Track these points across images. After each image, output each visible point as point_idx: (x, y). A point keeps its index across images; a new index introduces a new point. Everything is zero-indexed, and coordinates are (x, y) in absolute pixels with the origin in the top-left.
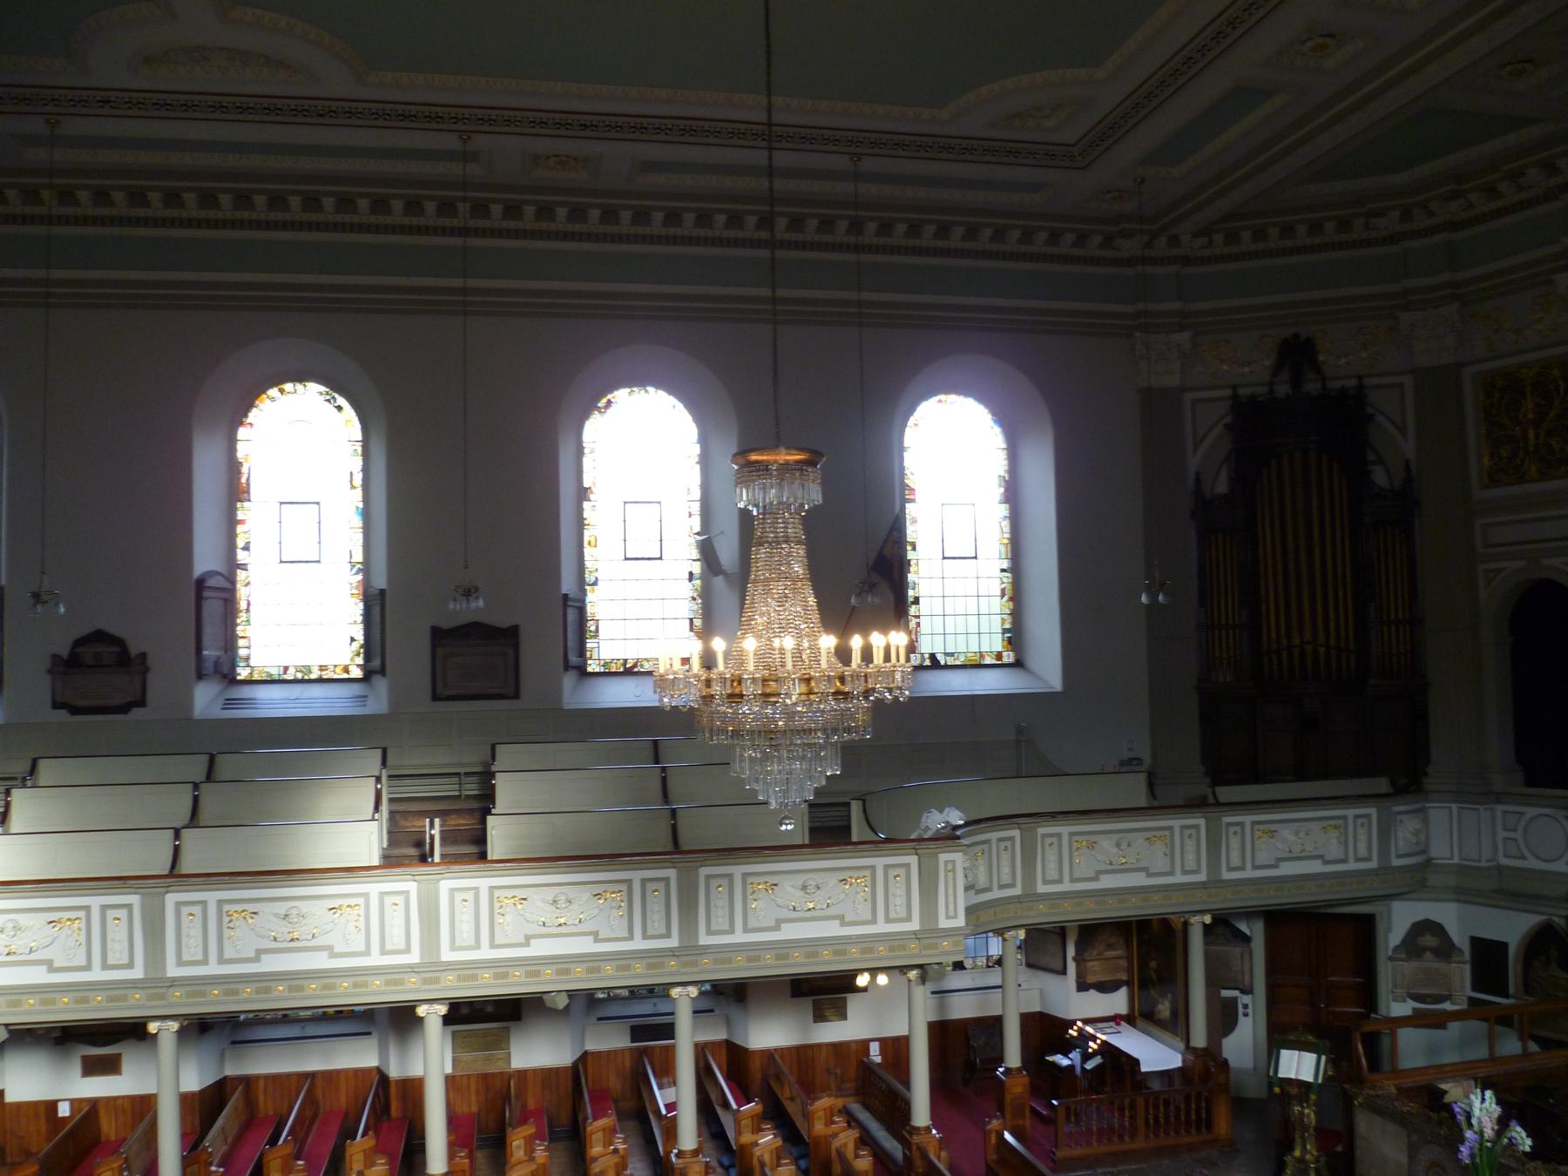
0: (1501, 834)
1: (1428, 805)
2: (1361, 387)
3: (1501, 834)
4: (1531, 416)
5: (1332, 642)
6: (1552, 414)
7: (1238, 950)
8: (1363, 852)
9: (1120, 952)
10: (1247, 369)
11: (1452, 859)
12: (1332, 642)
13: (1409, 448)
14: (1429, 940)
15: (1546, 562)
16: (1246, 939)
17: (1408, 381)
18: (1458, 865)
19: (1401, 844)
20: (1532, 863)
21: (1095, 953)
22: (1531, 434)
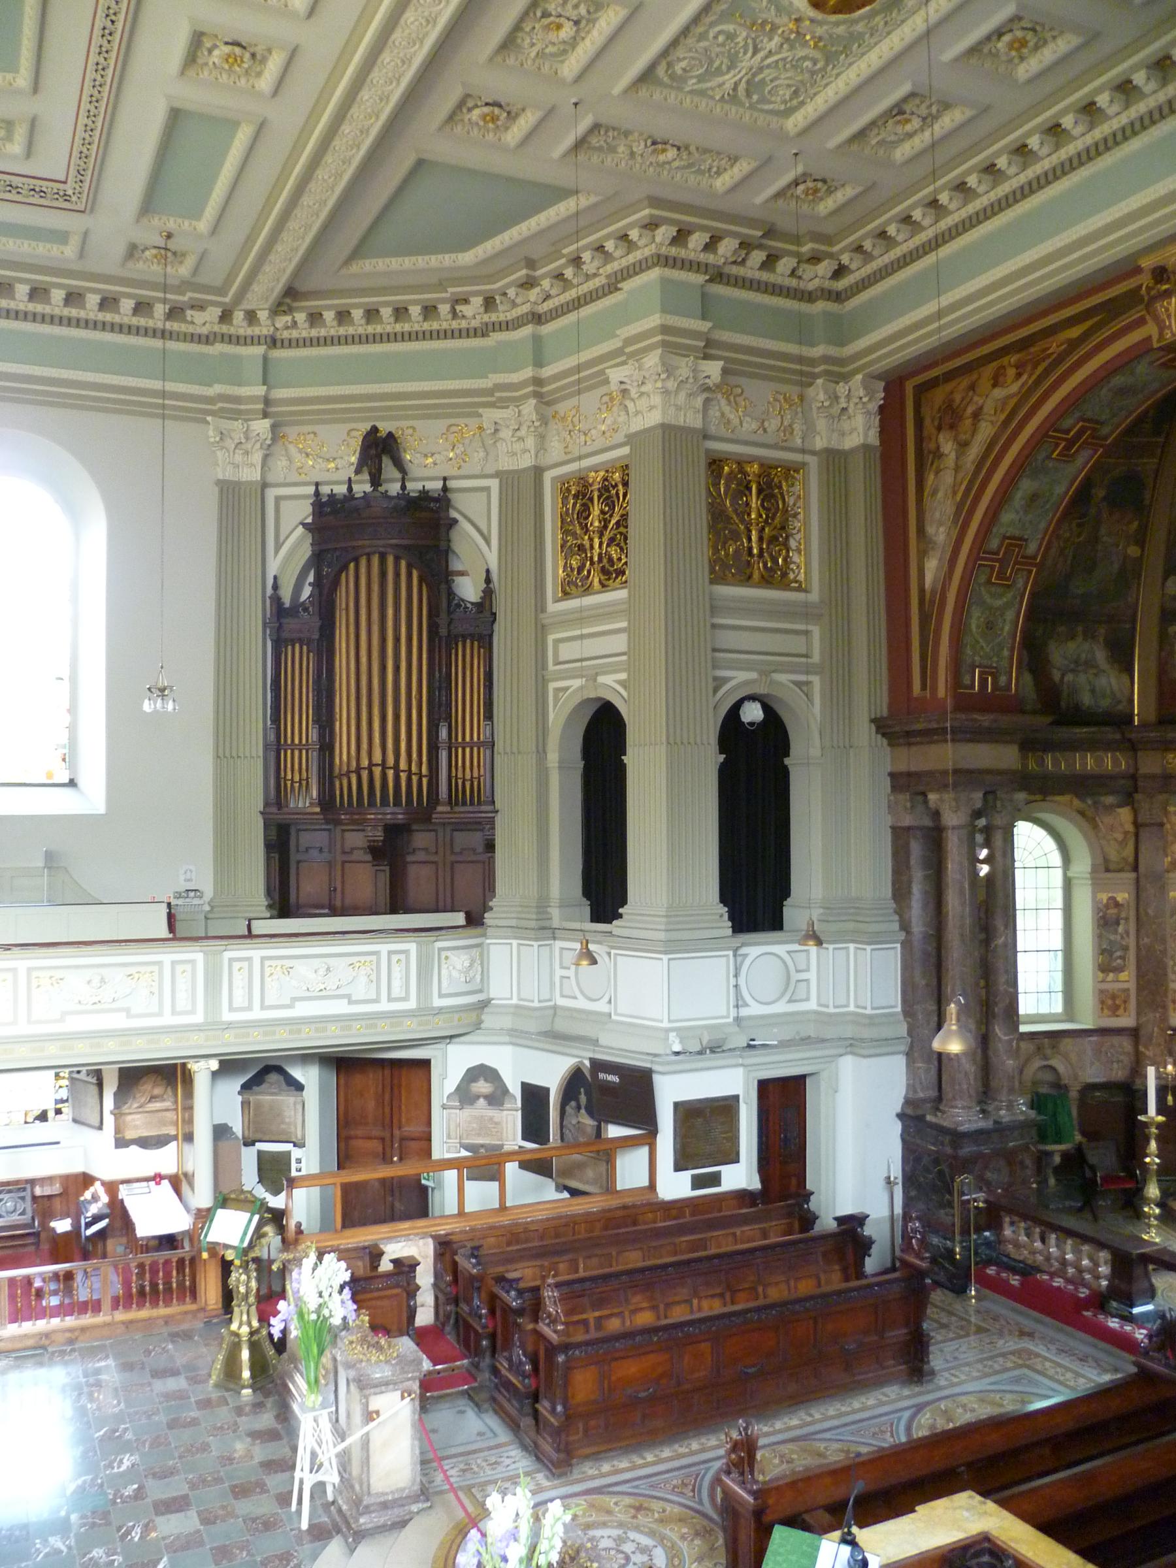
0: (559, 972)
1: (488, 941)
2: (445, 489)
3: (559, 972)
4: (596, 524)
5: (391, 761)
6: (613, 522)
7: (292, 1100)
8: (397, 991)
9: (168, 1104)
10: (332, 465)
11: (511, 998)
12: (403, 765)
13: (492, 558)
14: (482, 1086)
15: (602, 679)
16: (299, 1087)
17: (494, 484)
18: (517, 1006)
19: (445, 984)
20: (582, 1004)
21: (136, 1105)
22: (596, 541)
